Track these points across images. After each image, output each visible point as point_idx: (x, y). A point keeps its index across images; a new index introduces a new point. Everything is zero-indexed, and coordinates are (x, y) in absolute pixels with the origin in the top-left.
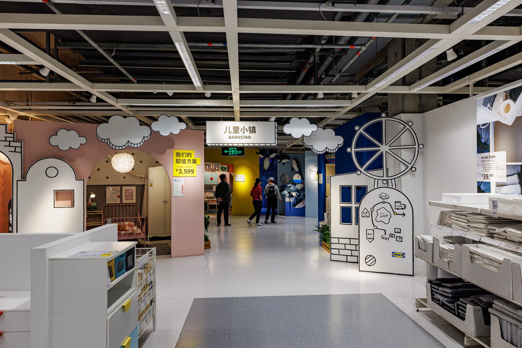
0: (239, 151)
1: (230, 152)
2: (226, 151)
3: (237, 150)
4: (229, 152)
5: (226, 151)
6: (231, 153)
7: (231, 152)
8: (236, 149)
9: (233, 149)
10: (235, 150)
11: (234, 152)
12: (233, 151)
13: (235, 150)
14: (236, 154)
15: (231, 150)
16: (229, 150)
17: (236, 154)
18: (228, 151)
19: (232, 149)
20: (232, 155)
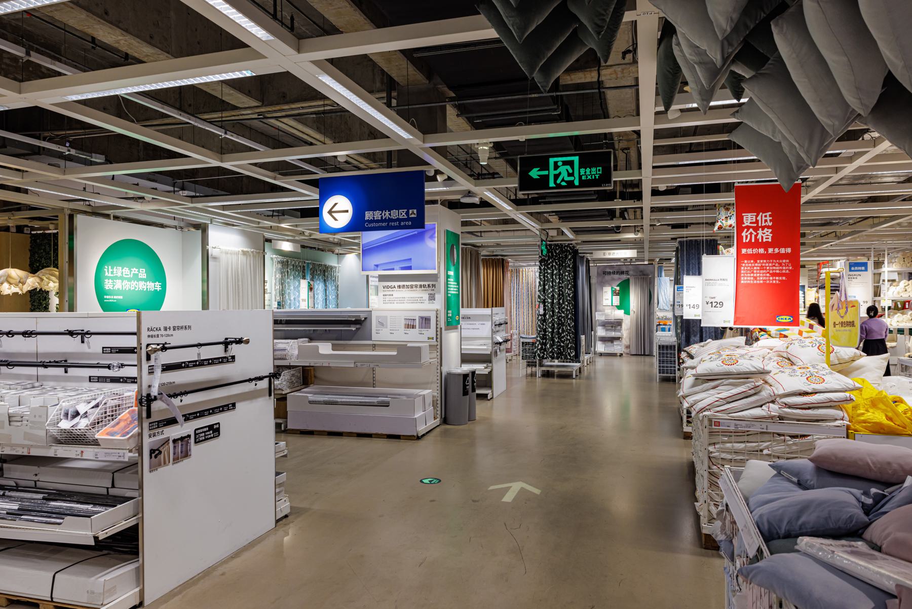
0: (588, 170)
1: (552, 172)
2: (535, 170)
3: (580, 168)
4: (547, 176)
5: (535, 173)
6: (556, 177)
7: (557, 172)
8: (576, 159)
9: (565, 163)
10: (571, 163)
11: (570, 175)
12: (563, 170)
13: (573, 168)
14: (577, 183)
15: (556, 167)
16: (548, 169)
17: (577, 183)
18: (546, 173)
19: (560, 164)
20: (559, 186)
